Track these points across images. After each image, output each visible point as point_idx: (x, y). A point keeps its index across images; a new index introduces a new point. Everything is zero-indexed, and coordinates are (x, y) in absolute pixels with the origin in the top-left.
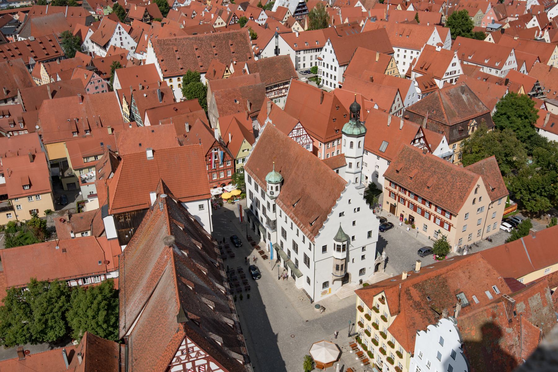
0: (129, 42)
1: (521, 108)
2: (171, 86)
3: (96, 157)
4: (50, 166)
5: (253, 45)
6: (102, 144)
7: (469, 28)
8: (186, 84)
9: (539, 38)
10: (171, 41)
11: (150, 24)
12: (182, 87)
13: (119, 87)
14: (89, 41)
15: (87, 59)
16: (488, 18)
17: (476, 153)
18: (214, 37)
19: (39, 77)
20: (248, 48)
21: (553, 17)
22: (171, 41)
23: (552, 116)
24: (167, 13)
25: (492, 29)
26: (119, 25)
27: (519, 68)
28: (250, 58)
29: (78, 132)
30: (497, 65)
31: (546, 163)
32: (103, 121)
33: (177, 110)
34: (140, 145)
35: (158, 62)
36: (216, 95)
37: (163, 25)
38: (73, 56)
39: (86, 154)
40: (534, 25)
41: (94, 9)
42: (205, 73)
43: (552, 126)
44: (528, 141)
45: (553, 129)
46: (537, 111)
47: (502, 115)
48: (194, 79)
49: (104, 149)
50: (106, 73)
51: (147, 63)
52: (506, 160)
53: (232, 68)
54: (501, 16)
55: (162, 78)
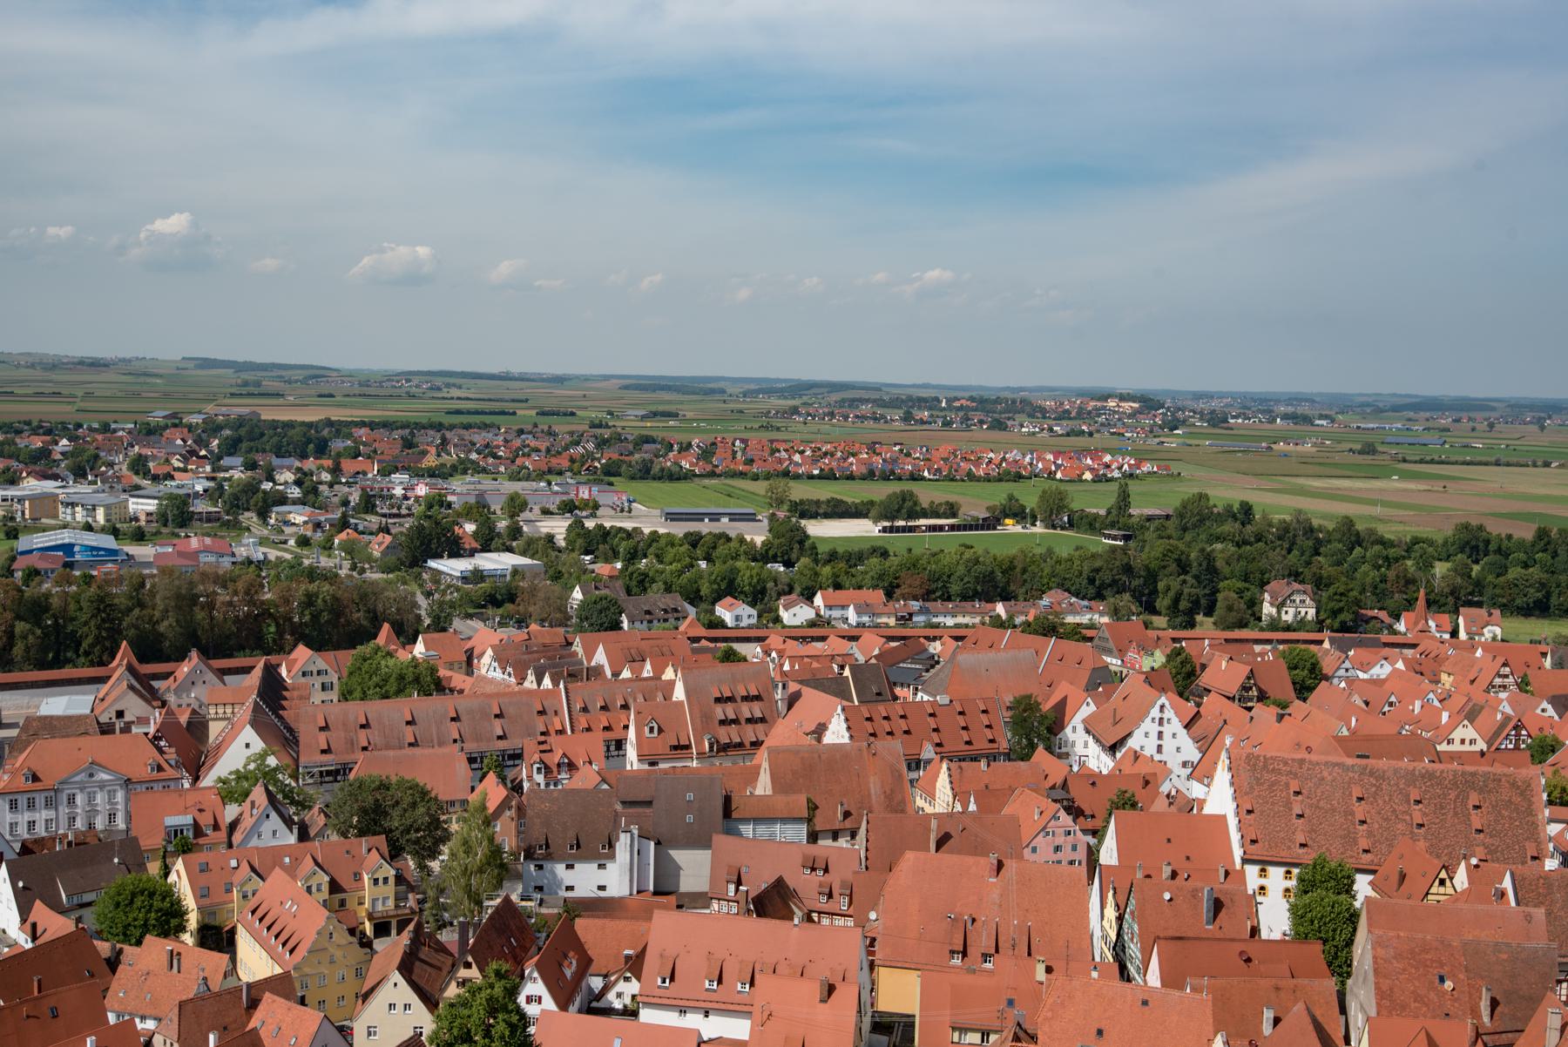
0: (1180, 747)
2: (1262, 888)
3: (985, 1035)
4: (866, 1026)
5: (1552, 820)
6: (1011, 1003)
8: (1306, 892)
10: (1286, 763)
11: (1250, 709)
12: (1292, 900)
13: (1114, 861)
14: (1080, 728)
15: (1055, 770)
18: (1423, 776)
19: (931, 795)
20: (1533, 831)
22: (1286, 763)
24: (1311, 689)
26: (1163, 700)
28: (1534, 858)
29: (964, 954)
32: (1035, 940)
33: (1249, 960)
34: (1100, 1032)
35: (1237, 814)
36: (1377, 944)
37: (1281, 717)
38: (1025, 757)
39: (961, 1021)
41: (1121, 653)
42: (1373, 872)
48: (1333, 883)
49: (1002, 1018)
50: (1093, 816)
51: (1207, 810)
53: (1461, 879)
55: (1238, 861)
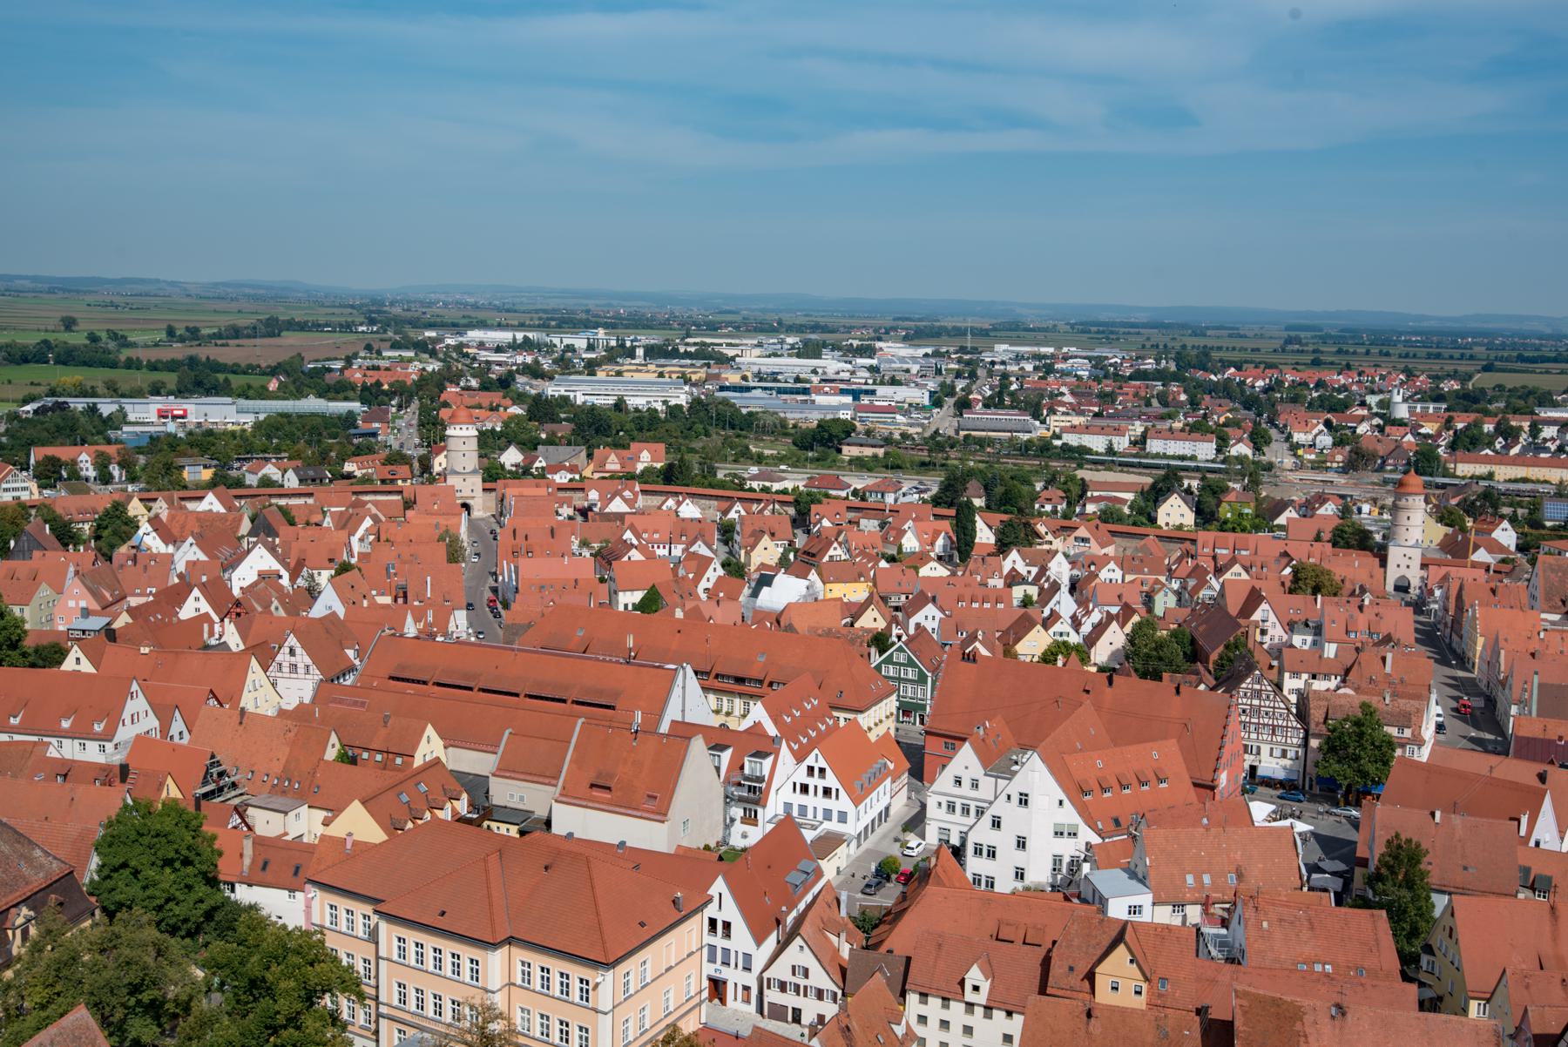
1: (164, 840)
7: (14, 638)
9: (213, 642)
16: (72, 604)
17: (43, 1007)
21: (245, 584)
23: (260, 842)
25: (84, 632)
27: (165, 728)
30: (98, 728)
31: (244, 983)
40: (197, 610)
43: (264, 868)
44: (208, 927)
45: (268, 875)
46: (214, 838)
47: (115, 870)
52: (139, 1002)
54: (107, 595)
